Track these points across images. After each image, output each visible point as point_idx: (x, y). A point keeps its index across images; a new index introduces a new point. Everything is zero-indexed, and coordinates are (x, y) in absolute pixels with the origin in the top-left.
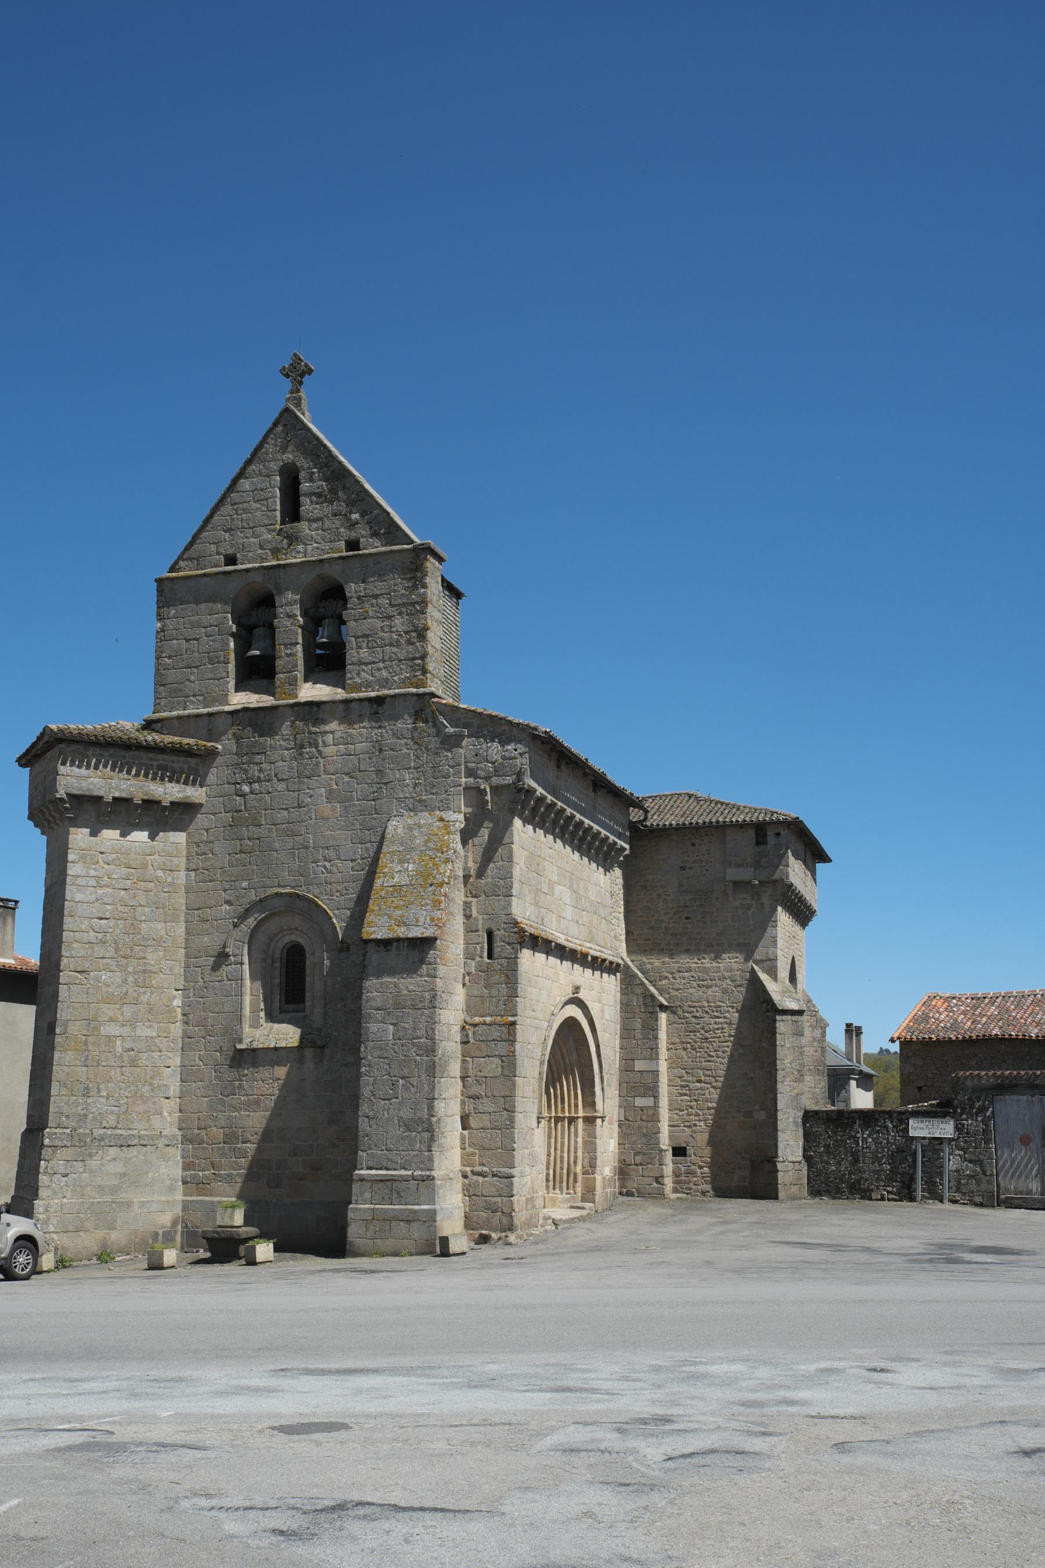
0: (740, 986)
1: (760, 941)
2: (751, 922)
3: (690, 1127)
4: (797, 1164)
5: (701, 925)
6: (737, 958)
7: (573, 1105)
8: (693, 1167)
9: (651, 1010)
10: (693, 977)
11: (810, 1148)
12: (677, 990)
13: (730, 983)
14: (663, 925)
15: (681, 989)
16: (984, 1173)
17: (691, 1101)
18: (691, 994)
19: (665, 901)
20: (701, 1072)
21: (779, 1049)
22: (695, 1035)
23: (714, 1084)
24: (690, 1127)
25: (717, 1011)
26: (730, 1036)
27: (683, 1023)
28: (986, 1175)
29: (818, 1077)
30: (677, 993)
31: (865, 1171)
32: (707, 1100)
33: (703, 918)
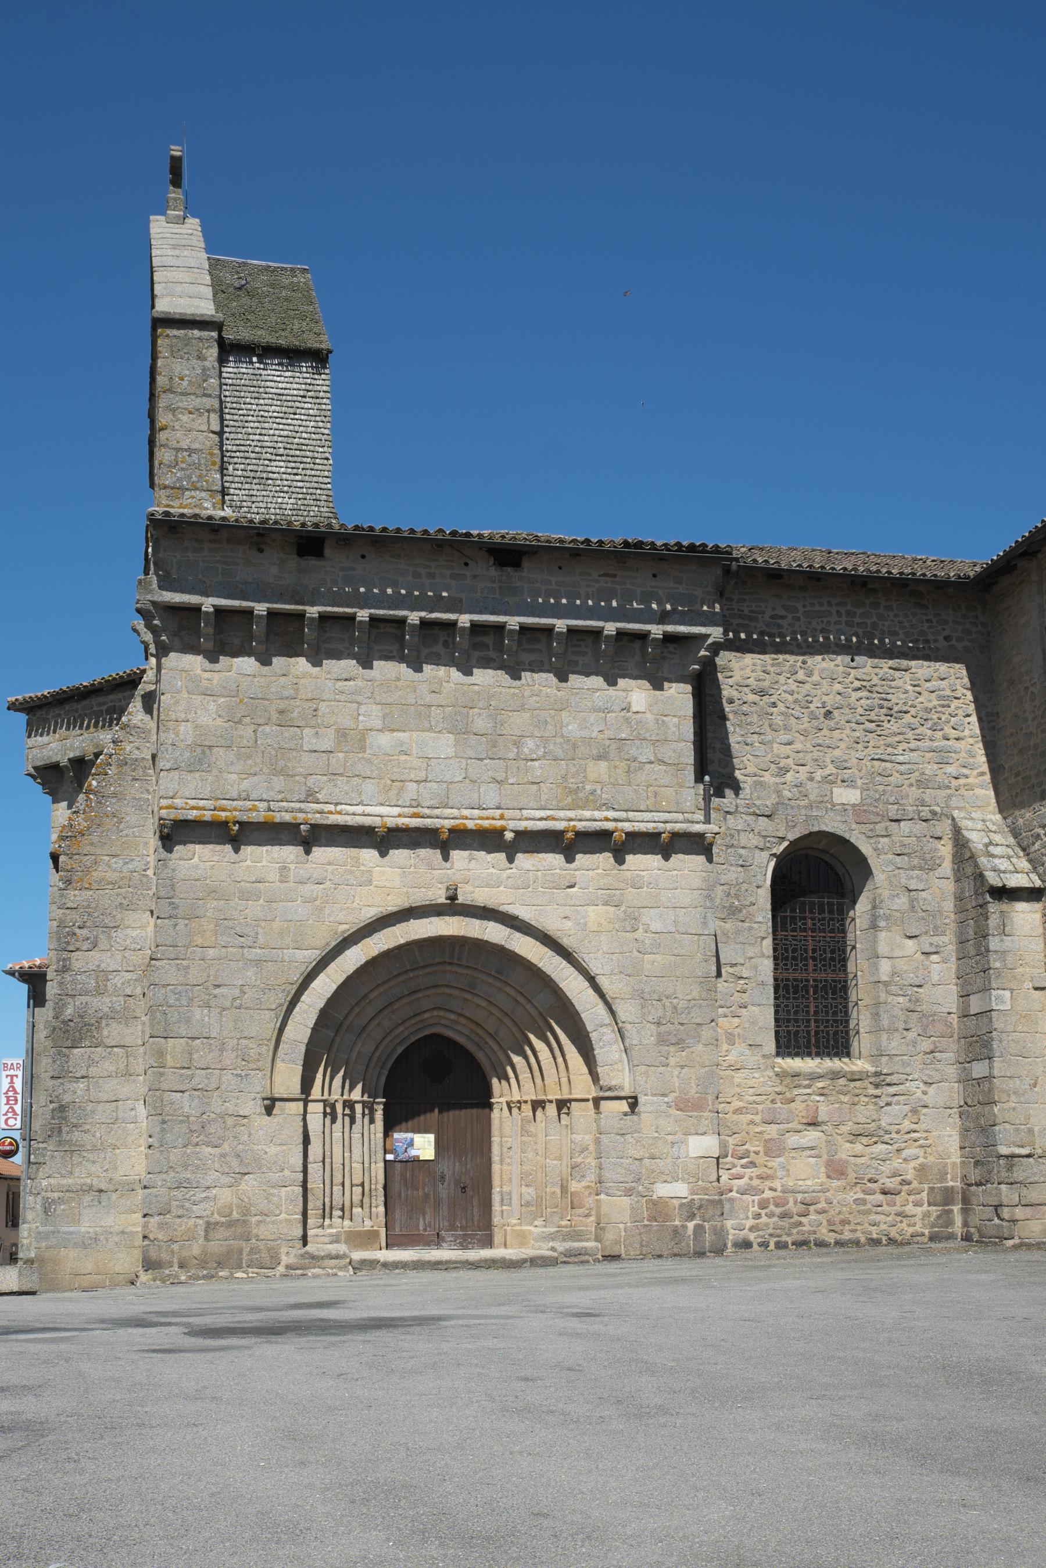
7: (564, 1080)
9: (981, 902)
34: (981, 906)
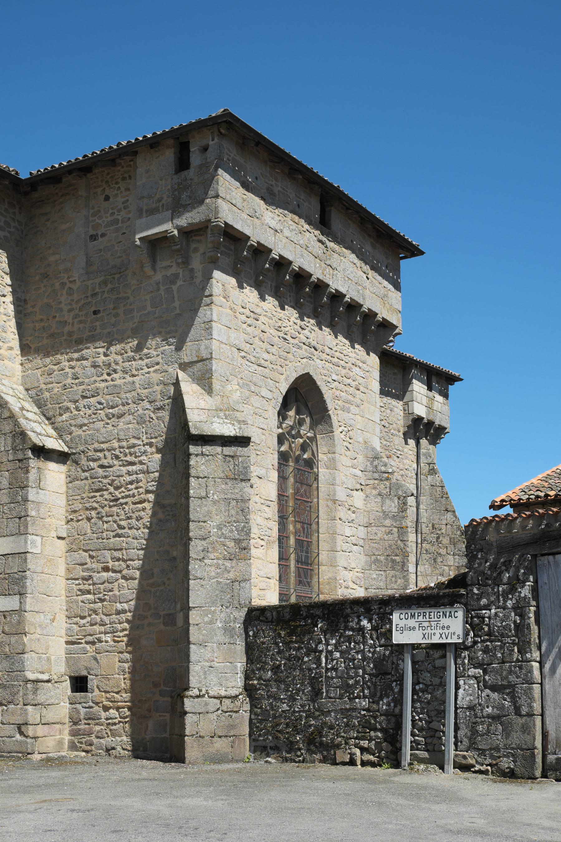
0: (161, 408)
1: (189, 331)
2: (177, 304)
3: (93, 643)
4: (227, 702)
5: (113, 320)
6: (158, 364)
8: (96, 708)
9: (20, 456)
10: (100, 403)
11: (253, 671)
12: (81, 426)
13: (148, 406)
14: (66, 330)
15: (85, 425)
16: (518, 712)
17: (95, 602)
18: (98, 430)
19: (70, 292)
20: (107, 554)
21: (193, 504)
22: (102, 496)
23: (125, 572)
24: (93, 643)
25: (131, 454)
26: (148, 492)
27: (86, 478)
28: (521, 715)
29: (392, 573)
30: (80, 432)
31: (329, 712)
32: (114, 601)
33: (114, 309)
34: (20, 461)
